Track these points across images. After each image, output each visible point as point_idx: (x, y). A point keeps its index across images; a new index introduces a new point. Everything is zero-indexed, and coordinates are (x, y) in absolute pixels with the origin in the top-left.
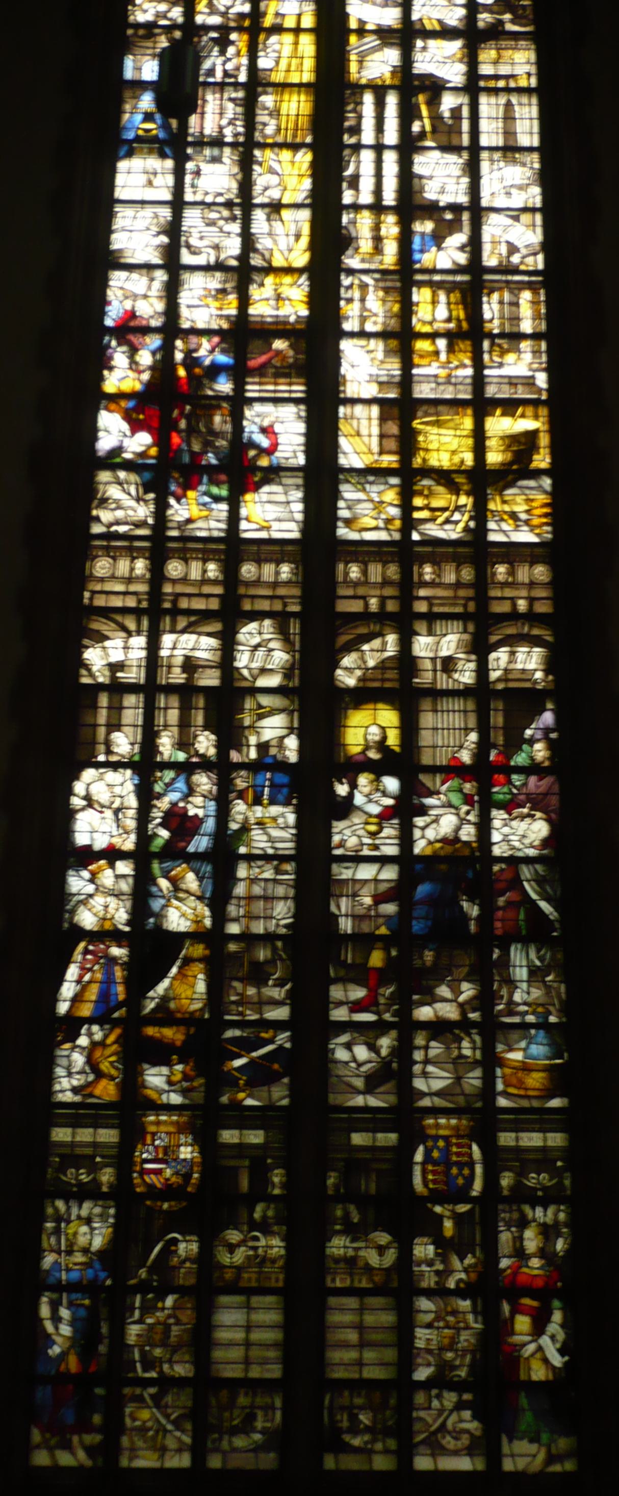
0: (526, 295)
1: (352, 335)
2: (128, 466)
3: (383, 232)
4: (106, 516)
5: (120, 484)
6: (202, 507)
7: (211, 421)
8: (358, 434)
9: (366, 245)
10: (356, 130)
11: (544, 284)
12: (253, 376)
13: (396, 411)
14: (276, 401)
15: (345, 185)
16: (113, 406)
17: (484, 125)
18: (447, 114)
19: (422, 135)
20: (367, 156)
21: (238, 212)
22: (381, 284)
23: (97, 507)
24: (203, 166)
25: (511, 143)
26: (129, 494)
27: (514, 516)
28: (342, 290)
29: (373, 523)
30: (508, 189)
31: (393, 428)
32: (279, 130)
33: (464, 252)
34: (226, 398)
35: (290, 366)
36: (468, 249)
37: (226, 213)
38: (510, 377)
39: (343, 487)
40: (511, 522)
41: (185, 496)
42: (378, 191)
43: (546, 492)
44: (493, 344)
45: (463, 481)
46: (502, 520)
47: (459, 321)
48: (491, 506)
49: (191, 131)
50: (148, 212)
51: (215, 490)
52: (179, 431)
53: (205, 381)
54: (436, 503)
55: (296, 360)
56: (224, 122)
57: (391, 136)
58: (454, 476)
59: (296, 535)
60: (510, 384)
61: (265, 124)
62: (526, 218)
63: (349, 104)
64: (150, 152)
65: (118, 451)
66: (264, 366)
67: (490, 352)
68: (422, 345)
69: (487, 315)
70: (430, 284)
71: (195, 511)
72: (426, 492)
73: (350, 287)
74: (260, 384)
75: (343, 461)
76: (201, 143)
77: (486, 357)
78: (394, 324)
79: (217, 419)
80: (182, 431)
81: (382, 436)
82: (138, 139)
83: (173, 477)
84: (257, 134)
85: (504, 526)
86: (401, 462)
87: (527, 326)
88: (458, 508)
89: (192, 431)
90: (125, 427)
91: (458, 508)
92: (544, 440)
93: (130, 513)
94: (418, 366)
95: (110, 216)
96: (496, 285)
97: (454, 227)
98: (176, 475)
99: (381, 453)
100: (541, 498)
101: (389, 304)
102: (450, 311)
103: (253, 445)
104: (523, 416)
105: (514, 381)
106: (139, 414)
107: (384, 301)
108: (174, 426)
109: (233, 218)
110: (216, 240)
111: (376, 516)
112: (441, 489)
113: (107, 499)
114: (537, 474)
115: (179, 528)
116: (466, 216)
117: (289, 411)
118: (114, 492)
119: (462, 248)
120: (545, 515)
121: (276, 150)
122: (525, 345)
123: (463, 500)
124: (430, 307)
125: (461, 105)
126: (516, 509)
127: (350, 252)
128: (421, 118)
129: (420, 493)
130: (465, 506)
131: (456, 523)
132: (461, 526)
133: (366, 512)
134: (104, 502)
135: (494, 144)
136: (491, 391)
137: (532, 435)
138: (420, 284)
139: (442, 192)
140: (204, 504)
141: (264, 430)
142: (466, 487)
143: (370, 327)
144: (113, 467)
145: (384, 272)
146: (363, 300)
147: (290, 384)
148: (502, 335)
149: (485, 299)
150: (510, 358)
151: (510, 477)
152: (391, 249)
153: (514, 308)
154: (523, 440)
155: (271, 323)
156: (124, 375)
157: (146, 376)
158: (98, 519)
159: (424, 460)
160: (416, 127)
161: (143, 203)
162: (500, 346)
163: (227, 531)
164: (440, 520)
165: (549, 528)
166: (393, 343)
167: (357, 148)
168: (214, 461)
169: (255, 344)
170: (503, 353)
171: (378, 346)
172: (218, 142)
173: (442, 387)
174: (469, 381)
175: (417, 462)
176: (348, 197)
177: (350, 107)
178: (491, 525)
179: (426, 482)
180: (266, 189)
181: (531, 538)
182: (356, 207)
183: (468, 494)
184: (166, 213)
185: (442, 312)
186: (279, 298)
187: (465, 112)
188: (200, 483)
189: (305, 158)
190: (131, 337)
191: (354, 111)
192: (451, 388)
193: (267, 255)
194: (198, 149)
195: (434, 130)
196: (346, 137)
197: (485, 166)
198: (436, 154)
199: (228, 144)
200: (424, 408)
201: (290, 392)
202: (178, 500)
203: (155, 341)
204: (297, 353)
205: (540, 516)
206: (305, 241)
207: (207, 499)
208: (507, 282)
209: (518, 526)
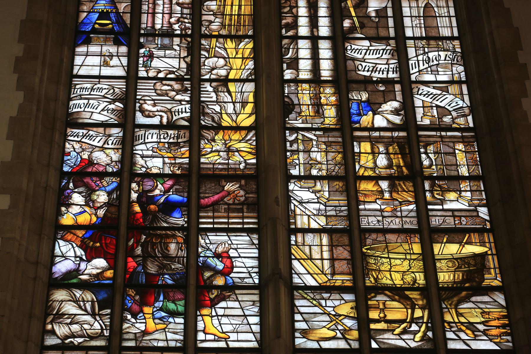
0: (461, 146)
1: (299, 178)
2: (84, 286)
3: (323, 100)
4: (61, 330)
5: (76, 301)
6: (157, 321)
7: (167, 248)
8: (311, 259)
9: (307, 111)
10: (295, 25)
11: (476, 138)
12: (207, 212)
13: (345, 240)
14: (227, 231)
15: (285, 66)
16: (69, 236)
17: (407, 22)
18: (373, 14)
19: (353, 29)
20: (304, 44)
21: (187, 84)
22: (323, 139)
23: (51, 322)
24: (156, 52)
25: (433, 34)
26: (86, 310)
27: (471, 326)
28: (288, 144)
29: (331, 334)
30: (434, 68)
31: (343, 253)
32: (223, 25)
33: (399, 115)
34: (181, 229)
35: (242, 204)
36: (402, 112)
37: (177, 86)
38: (453, 211)
39: (298, 303)
40: (469, 332)
41: (142, 311)
42: (316, 68)
43: (502, 306)
44: (432, 186)
45: (418, 297)
46: (461, 330)
47: (399, 166)
48: (448, 318)
49: (143, 26)
50: (104, 85)
51: (171, 306)
52: (134, 257)
53: (160, 215)
54: (390, 316)
55: (246, 199)
56: (173, 20)
57: (324, 30)
58: (407, 293)
59: (254, 345)
60: (454, 216)
61: (211, 22)
62: (453, 89)
63: (285, 7)
64: (106, 40)
65: (76, 272)
66: (216, 203)
67: (431, 191)
68: (366, 186)
69: (426, 163)
70: (369, 139)
71: (151, 325)
72: (381, 306)
73: (296, 140)
74: (213, 217)
75: (296, 280)
76: (152, 34)
77: (428, 194)
78: (338, 170)
79: (173, 247)
80: (139, 256)
81: (332, 260)
82: (94, 31)
83: (130, 296)
84: (203, 29)
85: (463, 336)
86: (354, 281)
87: (464, 171)
88: (413, 320)
89: (146, 256)
90: (80, 252)
91: (413, 320)
92: (492, 262)
93: (86, 326)
94: (365, 202)
95: (70, 87)
96: (431, 139)
97: (388, 96)
98: (132, 292)
99: (333, 274)
100: (496, 312)
101: (331, 155)
102: (390, 160)
103: (207, 267)
104: (469, 243)
105: (456, 213)
106: (95, 242)
107: (326, 152)
108: (130, 252)
109: (185, 90)
110: (169, 106)
111: (334, 327)
112: (396, 304)
113: (64, 314)
114: (489, 290)
115: (136, 339)
116: (398, 87)
117: (243, 239)
118: (70, 308)
119: (396, 112)
120: (504, 326)
121: (221, 40)
122: (464, 185)
123: (418, 313)
124: (370, 157)
125: (386, 7)
126: (472, 320)
127: (293, 116)
128: (350, 17)
129: (377, 308)
130: (422, 317)
131: (415, 333)
132: (419, 335)
133: (324, 324)
134: (59, 316)
135: (418, 34)
136: (435, 222)
137: (483, 255)
138: (360, 140)
139: (374, 70)
140: (161, 319)
141: (217, 256)
142: (420, 303)
143: (314, 172)
144: (69, 287)
145: (326, 130)
146: (308, 151)
147: (243, 218)
148: (439, 178)
149: (422, 150)
150: (452, 196)
151: (464, 293)
152: (330, 112)
153: (450, 157)
154: (472, 262)
155: (221, 169)
156: (81, 210)
157: (101, 213)
158: (53, 332)
159: (376, 279)
160: (347, 23)
161: (100, 77)
162: (440, 186)
163: (185, 341)
164: (397, 331)
165: (509, 338)
166: (338, 185)
167: (296, 38)
168: (170, 282)
169: (209, 186)
170: (444, 191)
171: (324, 187)
172: (169, 34)
173: (389, 220)
174: (414, 214)
175: (370, 282)
176: (288, 75)
177: (286, 10)
178: (450, 335)
179: (380, 298)
180: (213, 69)
181: (491, 346)
182: (296, 81)
183: (423, 308)
184: (121, 85)
185: (382, 161)
186: (229, 150)
187: (390, 12)
188: (157, 300)
189: (247, 46)
190: (87, 180)
191: (290, 12)
192: (397, 220)
193: (216, 119)
194: (150, 39)
195: (362, 26)
196: (284, 31)
197: (411, 52)
198: (366, 43)
199: (177, 36)
200: (374, 236)
201: (243, 223)
202: (134, 316)
203: (112, 183)
204: (247, 193)
205: (498, 327)
206: (249, 108)
207: (163, 314)
208: (441, 137)
209: (476, 336)
